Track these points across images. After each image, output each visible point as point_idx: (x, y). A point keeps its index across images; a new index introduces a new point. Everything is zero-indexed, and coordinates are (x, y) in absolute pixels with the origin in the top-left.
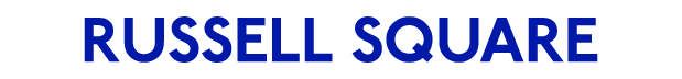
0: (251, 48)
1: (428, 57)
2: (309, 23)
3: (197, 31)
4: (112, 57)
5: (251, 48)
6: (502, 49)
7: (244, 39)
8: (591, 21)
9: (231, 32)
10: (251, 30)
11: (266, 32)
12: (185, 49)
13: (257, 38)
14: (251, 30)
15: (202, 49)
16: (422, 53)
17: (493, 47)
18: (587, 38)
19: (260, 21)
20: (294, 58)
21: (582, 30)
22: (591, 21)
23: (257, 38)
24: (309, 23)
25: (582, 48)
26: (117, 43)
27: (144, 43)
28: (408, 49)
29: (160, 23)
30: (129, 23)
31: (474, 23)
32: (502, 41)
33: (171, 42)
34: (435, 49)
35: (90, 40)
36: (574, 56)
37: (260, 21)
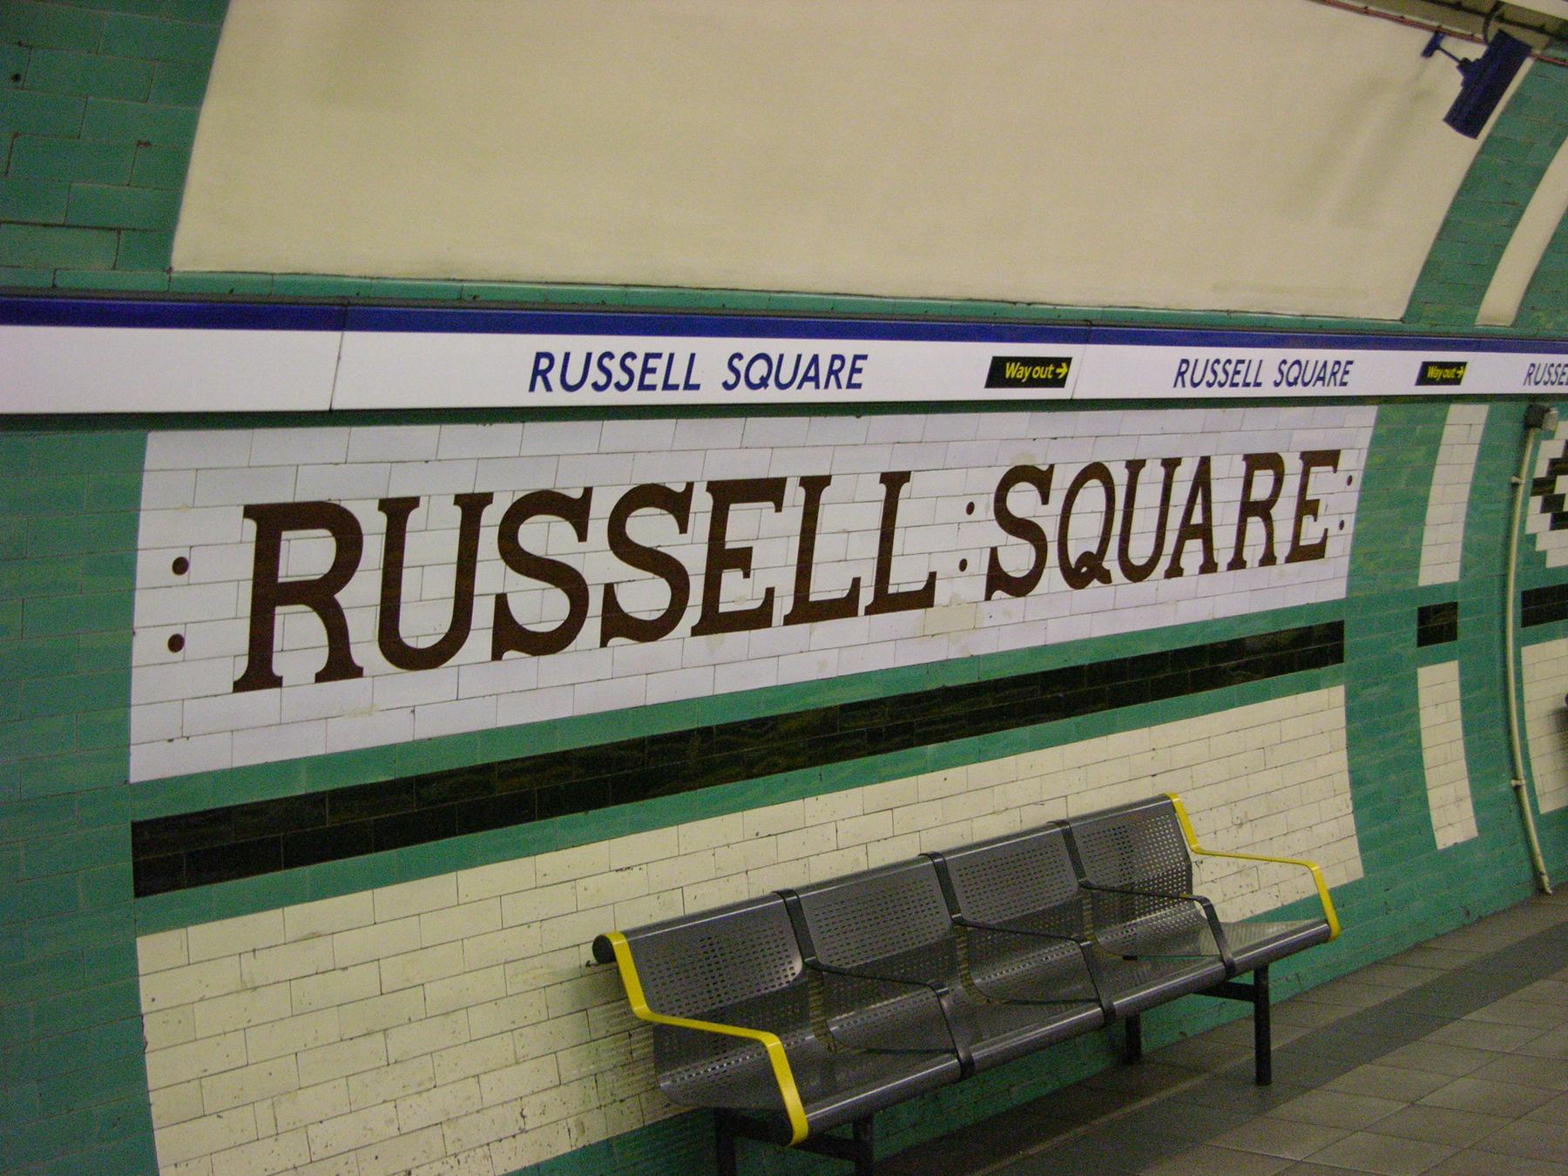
0: (649, 379)
1: (766, 386)
2: (693, 356)
3: (613, 365)
4: (548, 388)
5: (649, 379)
6: (811, 379)
7: (646, 370)
8: (864, 357)
9: (636, 366)
10: (652, 363)
11: (660, 365)
12: (602, 380)
13: (653, 371)
14: (652, 363)
15: (614, 381)
16: (764, 382)
17: (806, 378)
18: (860, 371)
19: (659, 356)
20: (676, 387)
21: (859, 364)
22: (864, 357)
23: (653, 371)
24: (693, 356)
25: (856, 379)
26: (554, 377)
27: (573, 377)
28: (755, 379)
29: (589, 355)
30: (567, 355)
31: (799, 357)
32: (812, 373)
33: (596, 375)
34: (771, 381)
35: (536, 372)
36: (850, 385)
37: (659, 356)
